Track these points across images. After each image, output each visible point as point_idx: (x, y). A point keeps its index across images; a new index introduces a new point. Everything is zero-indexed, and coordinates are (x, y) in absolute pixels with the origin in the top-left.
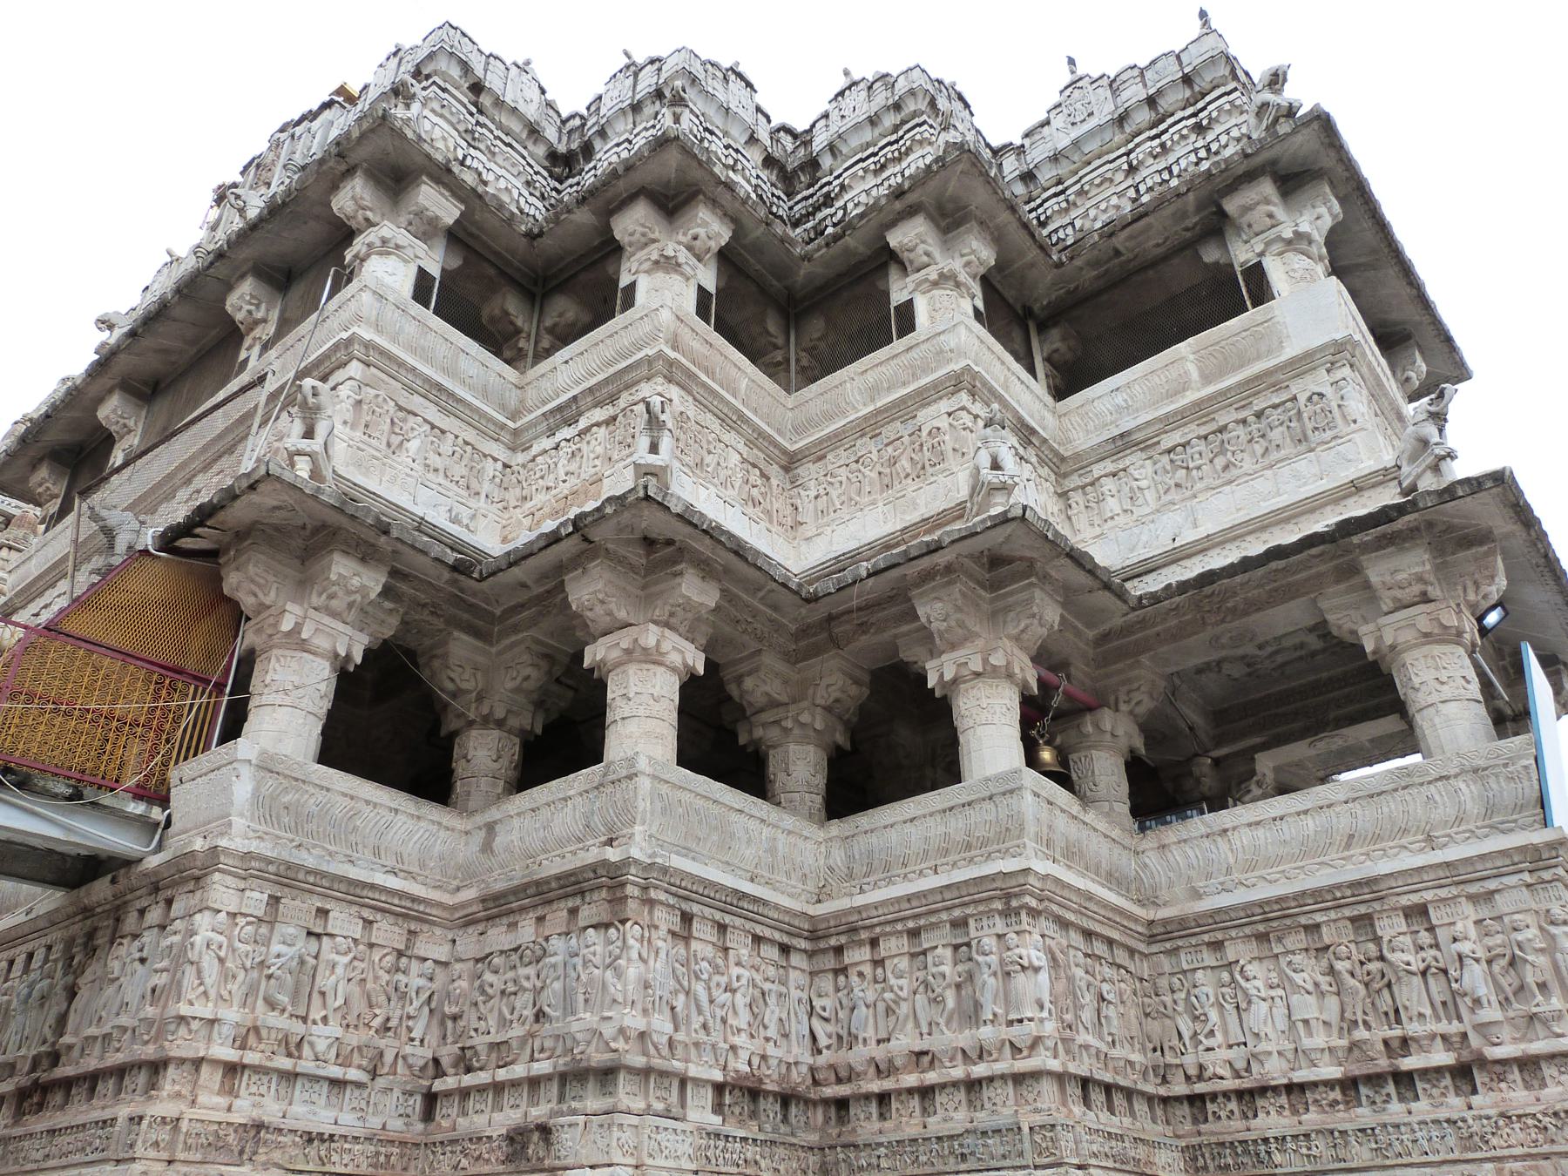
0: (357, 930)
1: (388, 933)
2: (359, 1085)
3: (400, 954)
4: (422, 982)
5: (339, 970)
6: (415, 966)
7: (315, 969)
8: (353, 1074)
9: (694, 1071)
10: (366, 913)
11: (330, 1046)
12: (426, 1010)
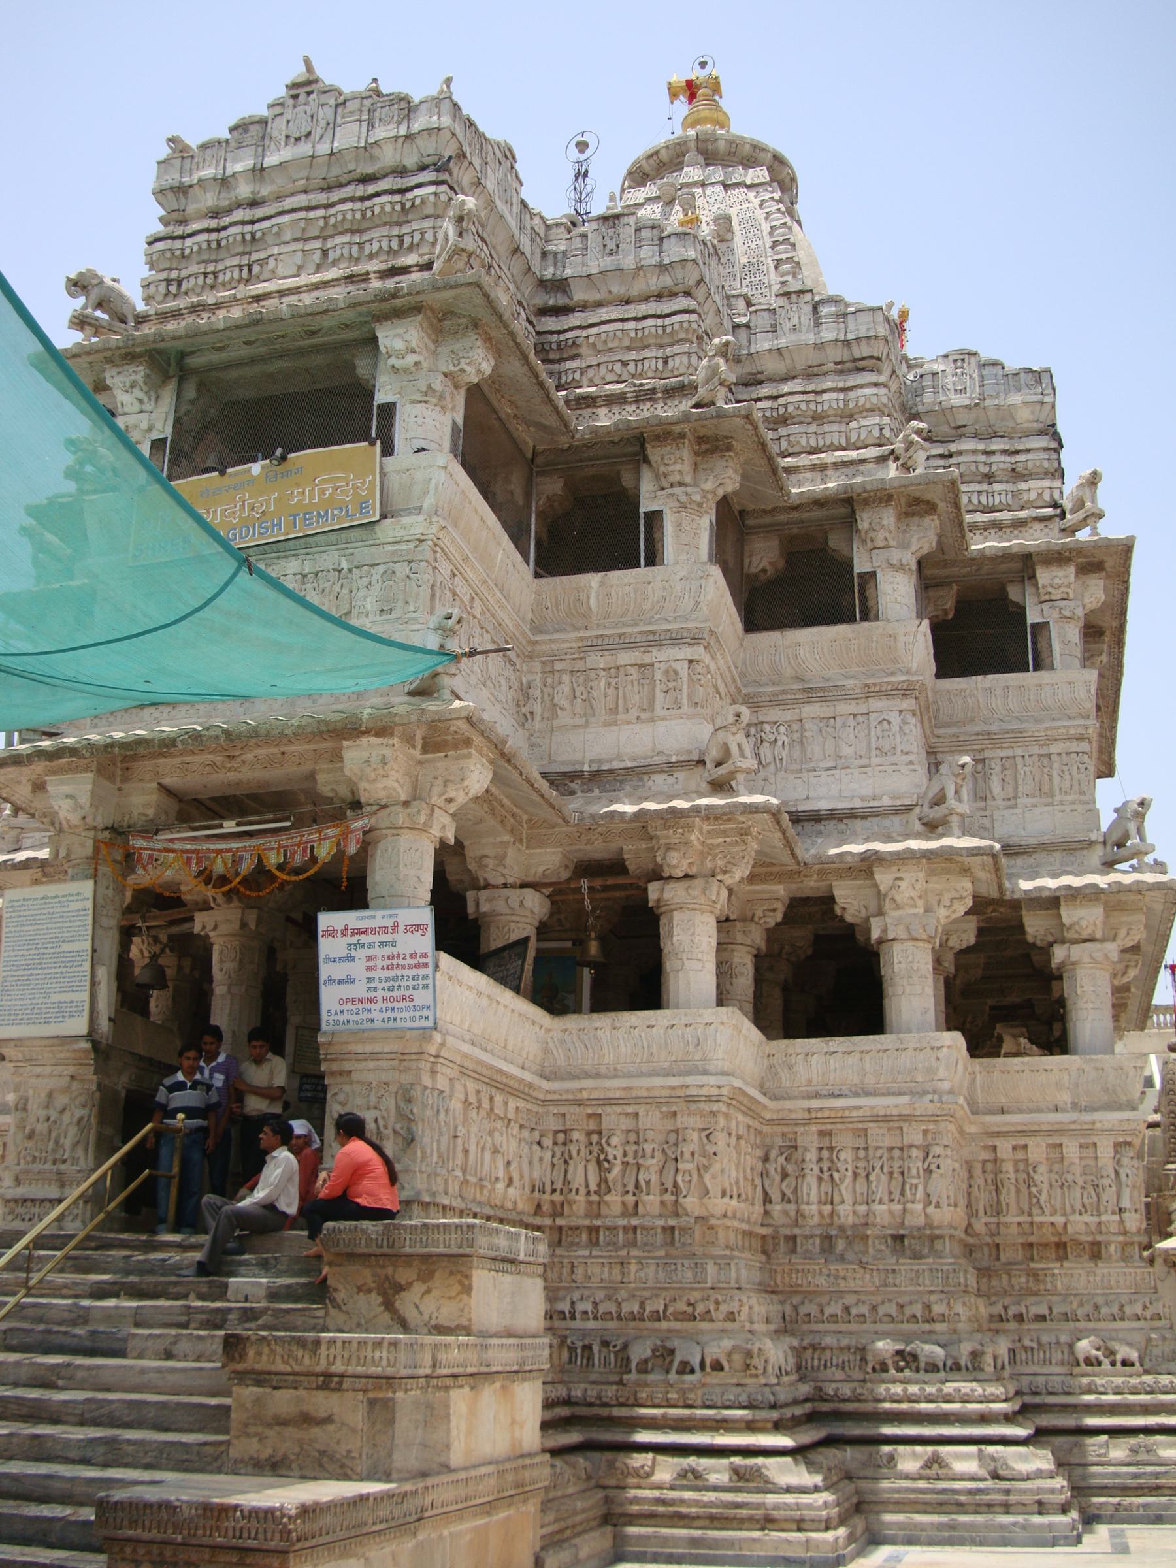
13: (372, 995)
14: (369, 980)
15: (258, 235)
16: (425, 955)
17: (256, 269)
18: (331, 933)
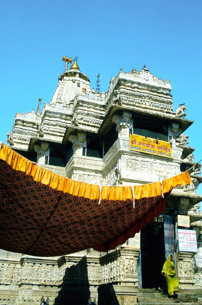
0: (8, 266)
1: (12, 265)
2: (10, 285)
3: (14, 268)
4: (17, 271)
5: (6, 271)
6: (16, 269)
7: (3, 271)
8: (8, 283)
9: (33, 283)
10: (9, 264)
11: (5, 280)
12: (18, 275)
13: (187, 245)
14: (187, 242)
15: (142, 95)
16: (195, 239)
17: (142, 102)
18: (180, 233)
